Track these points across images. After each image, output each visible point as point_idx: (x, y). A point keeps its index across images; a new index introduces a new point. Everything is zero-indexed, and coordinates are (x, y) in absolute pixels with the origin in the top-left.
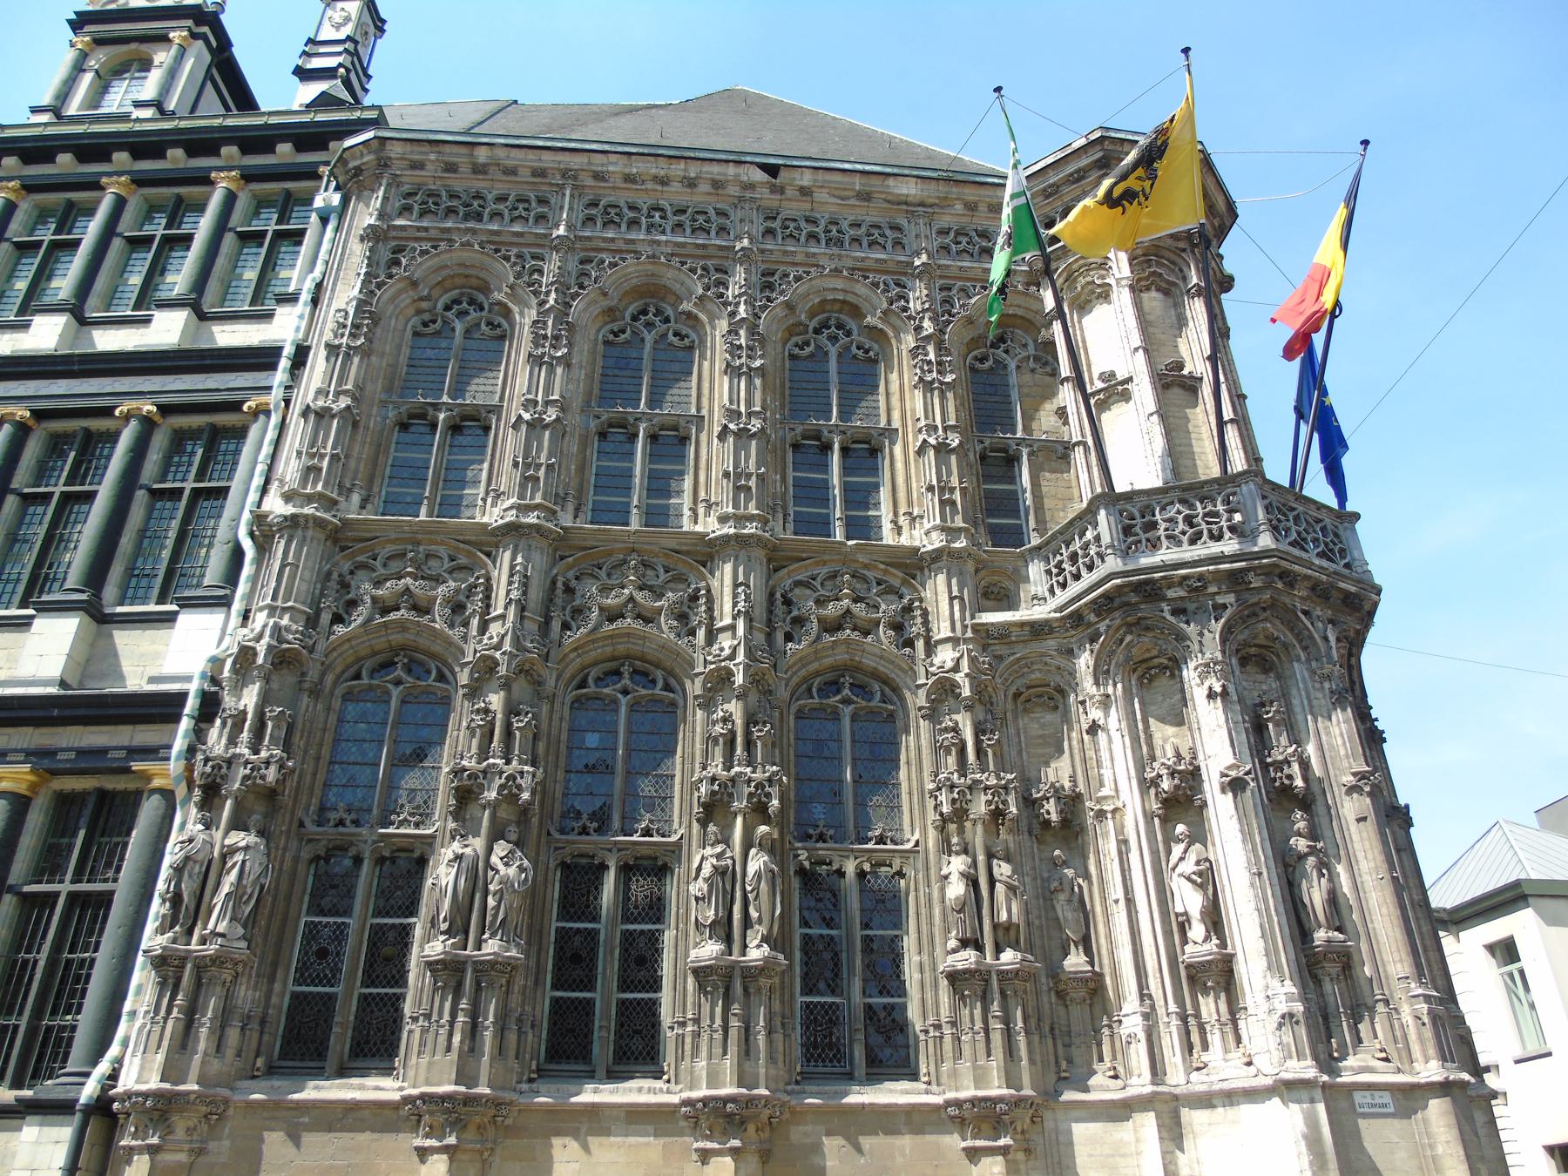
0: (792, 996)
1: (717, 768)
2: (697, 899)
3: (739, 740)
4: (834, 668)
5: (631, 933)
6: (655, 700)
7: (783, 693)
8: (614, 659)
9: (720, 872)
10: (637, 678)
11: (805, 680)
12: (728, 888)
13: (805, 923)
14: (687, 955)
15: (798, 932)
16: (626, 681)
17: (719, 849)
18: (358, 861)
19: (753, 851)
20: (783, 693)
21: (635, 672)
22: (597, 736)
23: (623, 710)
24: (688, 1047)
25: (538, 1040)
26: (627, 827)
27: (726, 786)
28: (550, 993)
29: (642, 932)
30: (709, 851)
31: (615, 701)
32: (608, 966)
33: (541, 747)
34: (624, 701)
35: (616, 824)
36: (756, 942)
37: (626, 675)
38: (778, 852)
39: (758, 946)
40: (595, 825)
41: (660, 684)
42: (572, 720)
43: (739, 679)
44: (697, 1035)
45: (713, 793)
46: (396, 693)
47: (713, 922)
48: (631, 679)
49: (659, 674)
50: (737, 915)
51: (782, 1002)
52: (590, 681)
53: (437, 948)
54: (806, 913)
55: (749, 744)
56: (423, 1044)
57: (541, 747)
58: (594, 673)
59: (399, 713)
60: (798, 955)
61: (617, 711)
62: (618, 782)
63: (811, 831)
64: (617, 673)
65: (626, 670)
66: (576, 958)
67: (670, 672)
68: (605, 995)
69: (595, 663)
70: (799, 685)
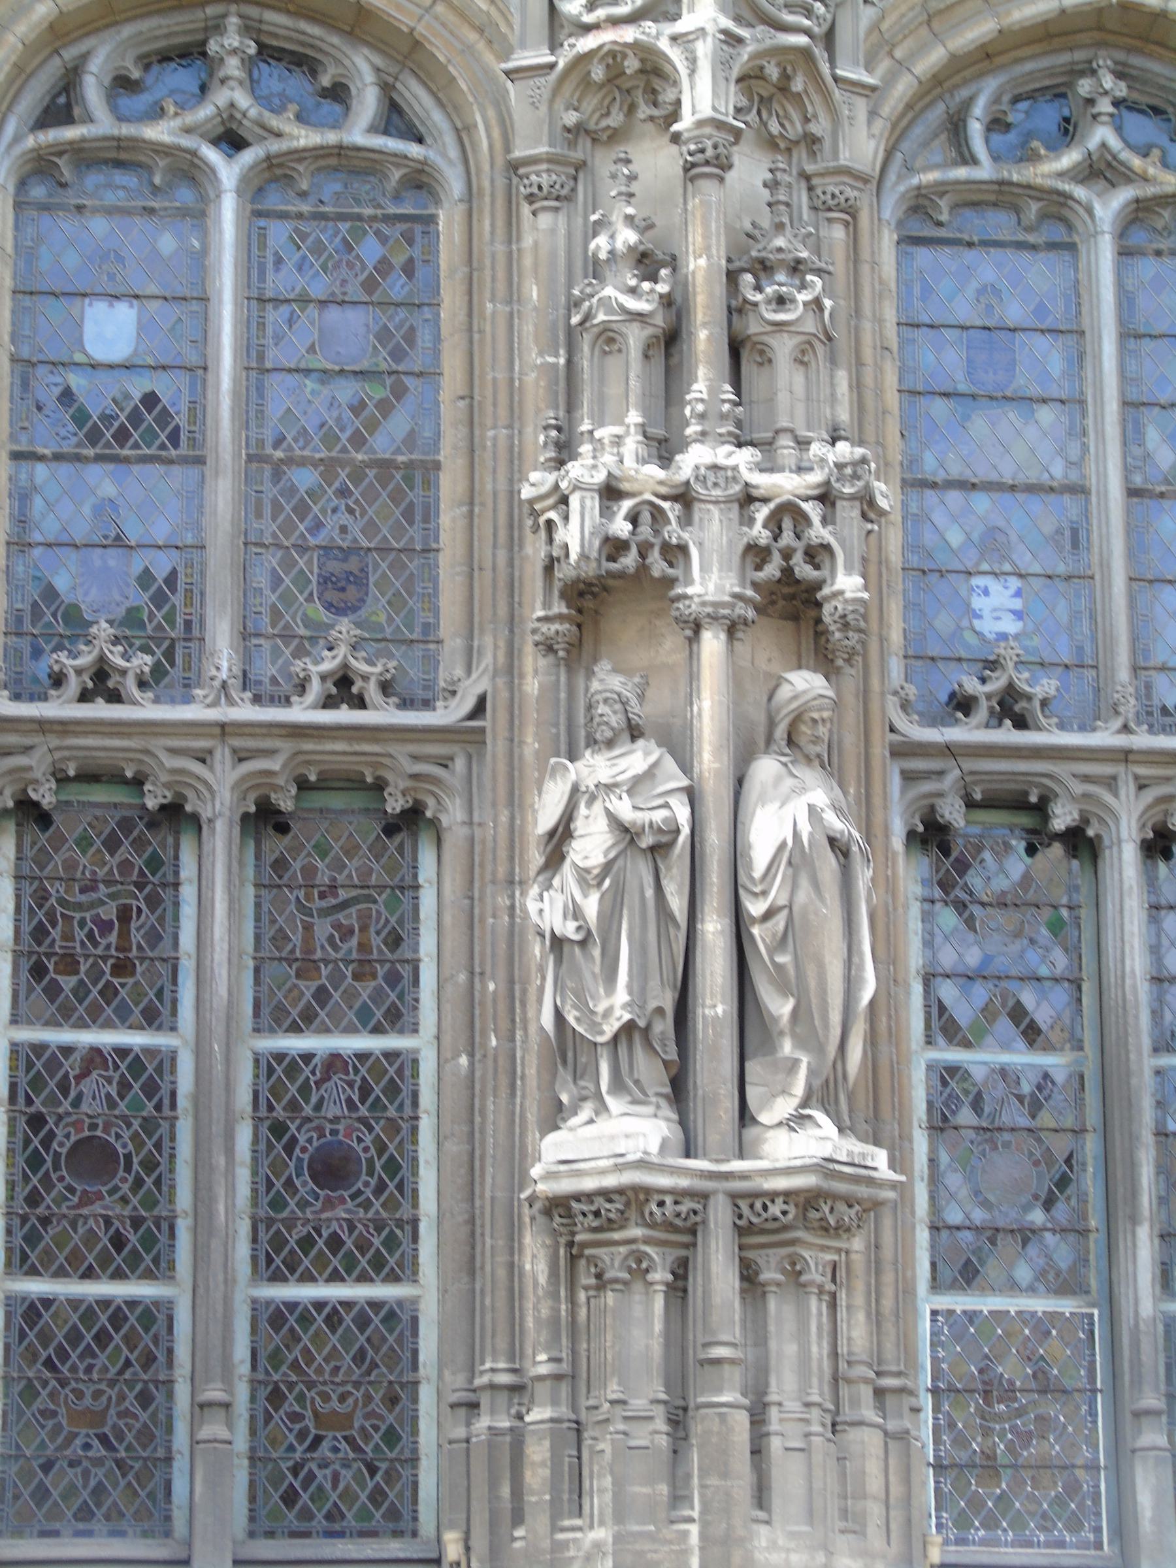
0: (906, 1292)
1: (614, 446)
2: (558, 943)
3: (705, 337)
5: (293, 1064)
6: (343, 161)
9: (642, 846)
10: (273, 78)
11: (937, 84)
12: (677, 904)
13: (943, 1025)
14: (518, 1160)
15: (920, 1061)
17: (636, 759)
19: (766, 768)
20: (861, 145)
21: (268, 52)
22: (125, 315)
23: (228, 211)
24: (537, 1476)
26: (265, 669)
27: (658, 515)
29: (335, 1062)
30: (595, 767)
31: (190, 171)
32: (217, 1179)
35: (223, 657)
36: (784, 1107)
37: (233, 67)
38: (852, 768)
39: (799, 1120)
40: (143, 662)
41: (368, 102)
42: (25, 253)
43: (701, 97)
44: (573, 1433)
45: (615, 547)
47: (629, 1028)
48: (252, 85)
49: (362, 69)
50: (715, 1004)
51: (876, 1320)
52: (92, 91)
54: (948, 991)
60: (921, 1144)
61: (199, 215)
63: (972, 686)
64: (191, 53)
66: (94, 1157)
67: (406, 53)
70: (914, 107)
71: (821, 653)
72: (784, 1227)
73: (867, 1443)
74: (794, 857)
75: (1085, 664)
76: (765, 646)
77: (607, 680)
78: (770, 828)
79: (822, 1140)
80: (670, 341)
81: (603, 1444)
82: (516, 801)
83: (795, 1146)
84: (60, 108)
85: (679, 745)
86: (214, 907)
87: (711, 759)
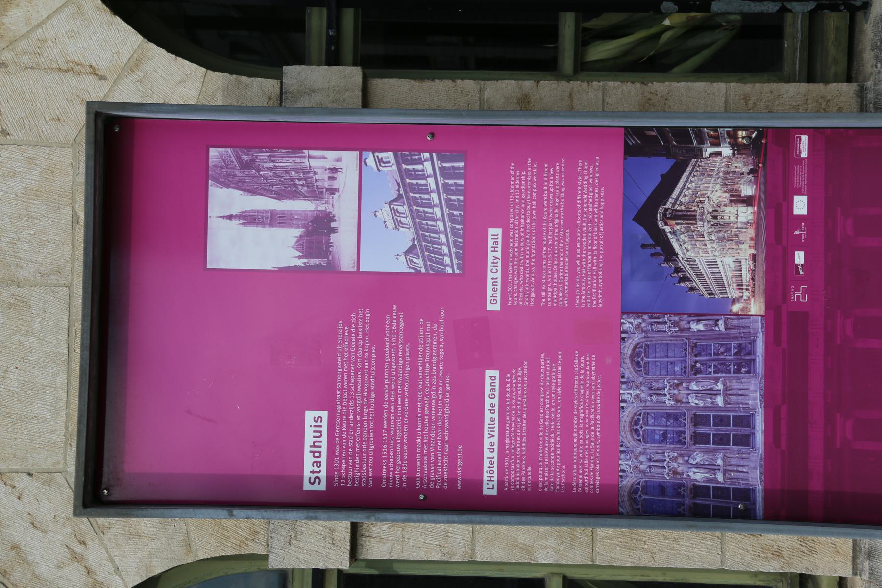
1: (666, 399)
4: (632, 363)
6: (643, 419)
7: (641, 379)
8: (631, 431)
15: (713, 375)
16: (638, 427)
18: (695, 504)
20: (641, 379)
25: (744, 449)
28: (731, 446)
32: (723, 430)
46: (644, 497)
49: (636, 417)
50: (709, 392)
53: (720, 477)
55: (658, 389)
56: (746, 480)
58: (636, 437)
65: (635, 427)
67: (635, 414)
68: (731, 430)
71: (681, 383)
72: (726, 389)
73: (743, 381)
76: (680, 388)
77: (684, 400)
79: (719, 384)
83: (720, 386)
84: (640, 440)
85: (689, 394)
86: (702, 430)
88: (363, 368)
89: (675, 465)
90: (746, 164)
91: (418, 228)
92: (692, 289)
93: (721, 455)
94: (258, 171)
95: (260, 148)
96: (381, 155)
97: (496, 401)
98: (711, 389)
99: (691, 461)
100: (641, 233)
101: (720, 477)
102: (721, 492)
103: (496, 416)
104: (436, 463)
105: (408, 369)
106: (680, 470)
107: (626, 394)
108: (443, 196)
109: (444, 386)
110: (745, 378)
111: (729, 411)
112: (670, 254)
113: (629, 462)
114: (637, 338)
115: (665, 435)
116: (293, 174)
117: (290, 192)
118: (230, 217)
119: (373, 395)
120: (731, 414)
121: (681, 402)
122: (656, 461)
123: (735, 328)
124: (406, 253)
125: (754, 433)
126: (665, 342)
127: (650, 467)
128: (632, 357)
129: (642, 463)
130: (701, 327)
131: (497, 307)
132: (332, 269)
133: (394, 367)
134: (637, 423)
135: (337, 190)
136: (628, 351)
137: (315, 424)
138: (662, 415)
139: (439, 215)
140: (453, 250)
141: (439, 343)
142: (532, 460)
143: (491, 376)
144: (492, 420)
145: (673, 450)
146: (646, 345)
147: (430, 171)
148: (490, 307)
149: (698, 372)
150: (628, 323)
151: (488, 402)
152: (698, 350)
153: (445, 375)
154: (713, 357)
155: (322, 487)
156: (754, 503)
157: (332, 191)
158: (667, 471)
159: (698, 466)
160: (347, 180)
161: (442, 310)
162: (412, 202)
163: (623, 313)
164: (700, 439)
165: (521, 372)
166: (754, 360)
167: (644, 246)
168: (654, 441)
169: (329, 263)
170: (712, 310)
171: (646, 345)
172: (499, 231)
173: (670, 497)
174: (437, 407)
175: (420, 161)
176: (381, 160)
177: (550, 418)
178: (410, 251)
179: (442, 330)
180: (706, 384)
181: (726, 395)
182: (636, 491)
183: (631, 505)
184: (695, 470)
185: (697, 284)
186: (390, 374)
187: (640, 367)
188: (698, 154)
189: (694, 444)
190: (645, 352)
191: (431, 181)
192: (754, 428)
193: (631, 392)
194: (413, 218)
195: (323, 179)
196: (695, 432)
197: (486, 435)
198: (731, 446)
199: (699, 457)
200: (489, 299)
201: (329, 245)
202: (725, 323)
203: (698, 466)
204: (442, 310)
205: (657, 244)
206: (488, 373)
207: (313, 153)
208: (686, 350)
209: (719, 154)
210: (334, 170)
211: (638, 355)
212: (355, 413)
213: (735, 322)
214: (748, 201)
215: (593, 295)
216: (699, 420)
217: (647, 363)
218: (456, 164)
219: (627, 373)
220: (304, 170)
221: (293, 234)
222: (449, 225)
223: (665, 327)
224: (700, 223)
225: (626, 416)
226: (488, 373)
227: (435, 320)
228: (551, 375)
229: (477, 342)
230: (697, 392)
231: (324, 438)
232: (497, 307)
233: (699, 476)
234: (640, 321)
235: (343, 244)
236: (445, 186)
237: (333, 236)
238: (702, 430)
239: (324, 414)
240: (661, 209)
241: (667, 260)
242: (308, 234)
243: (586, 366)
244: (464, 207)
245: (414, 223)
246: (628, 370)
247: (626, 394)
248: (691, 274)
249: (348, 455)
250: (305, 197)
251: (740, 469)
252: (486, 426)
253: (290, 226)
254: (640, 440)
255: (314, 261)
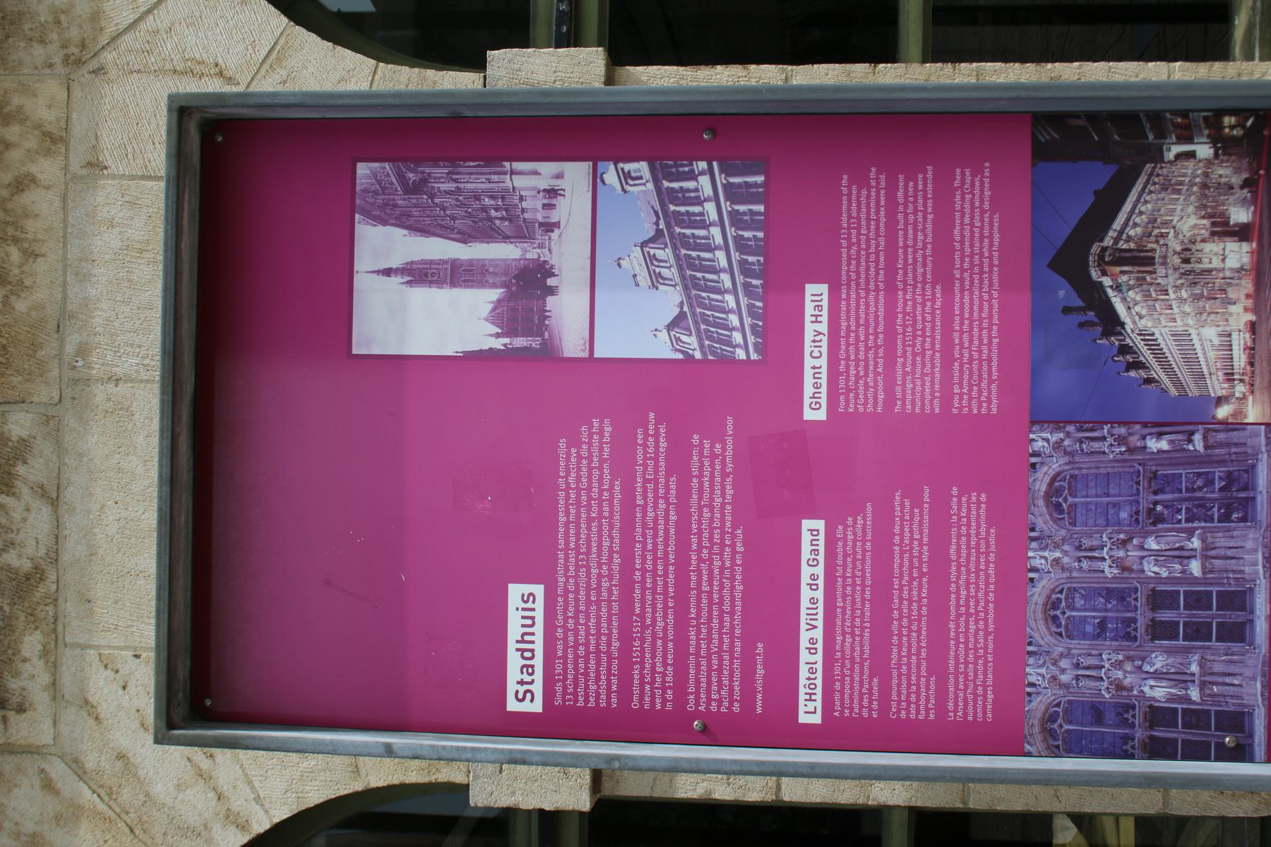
1: (1105, 566)
4: (1047, 507)
6: (1067, 598)
7: (1063, 532)
8: (1046, 620)
9: (1157, 563)
16: (1058, 613)
17: (1145, 563)
18: (1151, 737)
20: (1063, 532)
25: (1236, 646)
31: (1069, 618)
32: (1201, 615)
33: (1094, 652)
34: (1068, 613)
43: (1057, 554)
46: (1066, 727)
49: (1054, 596)
50: (1177, 553)
53: (1194, 694)
55: (1091, 549)
57: (1094, 652)
58: (1054, 629)
59: (1077, 724)
60: (1195, 525)
62: (1110, 614)
65: (1052, 613)
67: (1053, 591)
68: (1214, 616)
69: (1048, 628)
71: (1131, 539)
72: (1207, 547)
73: (1235, 533)
74: (1158, 543)
75: (1131, 503)
76: (1129, 547)
77: (1135, 567)
78: (1155, 547)
80: (1091, 558)
81: (1235, 568)
82: (1151, 578)
83: (1196, 543)
85: (1143, 558)
86: (1165, 616)
87: (1145, 553)
88: (600, 516)
89: (1120, 674)
90: (1237, 171)
91: (689, 285)
92: (1149, 381)
93: (1196, 657)
94: (432, 196)
95: (435, 161)
96: (628, 167)
97: (820, 570)
98: (1181, 548)
99: (1147, 668)
100: (1064, 293)
101: (1194, 694)
102: (1195, 718)
103: (820, 594)
104: (720, 670)
105: (673, 518)
106: (1127, 682)
107: (1037, 557)
108: (731, 232)
109: (733, 545)
110: (1238, 530)
111: (1211, 584)
112: (1112, 324)
113: (1043, 671)
114: (1056, 464)
115: (1102, 625)
116: (487, 201)
117: (482, 231)
118: (387, 272)
119: (617, 560)
120: (1214, 589)
121: (1130, 569)
122: (1088, 668)
123: (1221, 445)
124: (671, 326)
125: (1252, 621)
126: (1103, 471)
127: (1077, 678)
128: (1047, 496)
129: (1063, 671)
130: (1164, 445)
131: (821, 415)
132: (548, 355)
133: (651, 514)
134: (1055, 605)
135: (557, 225)
136: (1041, 486)
137: (523, 605)
138: (1097, 592)
139: (723, 263)
140: (748, 321)
141: (724, 475)
142: (880, 665)
143: (812, 530)
144: (813, 601)
145: (1117, 651)
146: (1072, 476)
147: (708, 191)
148: (809, 415)
149: (1159, 519)
150: (1041, 440)
151: (806, 572)
152: (1160, 483)
153: (734, 527)
154: (1184, 494)
155: (537, 707)
156: (1251, 736)
157: (549, 227)
158: (1105, 684)
159: (1157, 675)
160: (574, 209)
161: (730, 421)
162: (679, 243)
163: (1033, 423)
164: (1160, 631)
165: (864, 522)
166: (1254, 499)
167: (1067, 310)
168: (1084, 636)
169: (544, 344)
170: (1184, 415)
171: (1072, 476)
172: (823, 288)
173: (1110, 726)
174: (723, 581)
175: (692, 176)
176: (627, 176)
177: (911, 596)
178: (677, 322)
179: (729, 453)
180: (1173, 539)
181: (1205, 558)
182: (1053, 718)
183: (1045, 740)
184: (1152, 682)
185: (1158, 372)
186: (644, 526)
187: (1062, 512)
188: (1158, 157)
189: (1152, 640)
190: (1070, 488)
191: (710, 208)
192: (1252, 612)
193: (1046, 554)
194: (680, 268)
195: (533, 207)
196: (1153, 620)
197: (803, 626)
198: (1213, 643)
199: (1159, 662)
200: (807, 401)
201: (543, 315)
202: (1205, 438)
203: (1157, 675)
204: (730, 421)
205: (1089, 307)
206: (807, 524)
207: (518, 166)
208: (1138, 483)
209: (1192, 155)
210: (552, 193)
211: (1058, 492)
212: (588, 589)
213: (1222, 436)
214: (1242, 233)
215: (981, 394)
216: (1160, 599)
217: (1073, 506)
218: (750, 179)
219: (1040, 523)
220: (504, 195)
221: (485, 298)
222: (740, 279)
223: (1104, 446)
224: (1161, 271)
225: (1037, 594)
226: (807, 524)
227: (719, 437)
228: (912, 527)
229: (789, 473)
230: (1157, 553)
231: (539, 629)
232: (821, 415)
233: (1159, 692)
234: (1061, 435)
235: (567, 311)
236: (734, 215)
237: (550, 300)
238: (1165, 616)
239: (539, 590)
240: (1095, 248)
241: (1106, 334)
242: (510, 297)
243: (971, 513)
244: (764, 248)
245: (683, 277)
246: (1041, 518)
247: (1037, 557)
248: (1147, 356)
249: (577, 657)
250: (506, 238)
251: (1228, 680)
252: (803, 612)
253: (482, 284)
254: (1060, 634)
255: (520, 342)
